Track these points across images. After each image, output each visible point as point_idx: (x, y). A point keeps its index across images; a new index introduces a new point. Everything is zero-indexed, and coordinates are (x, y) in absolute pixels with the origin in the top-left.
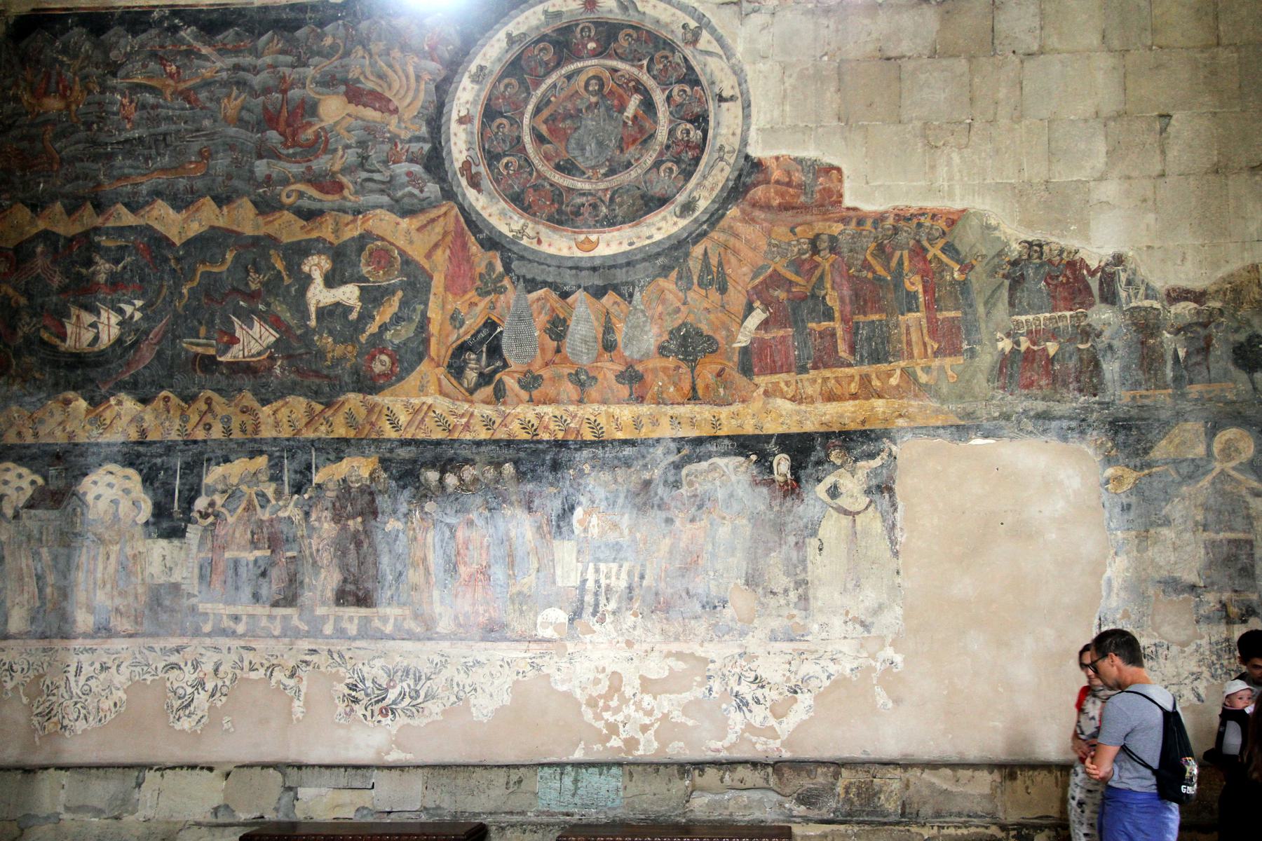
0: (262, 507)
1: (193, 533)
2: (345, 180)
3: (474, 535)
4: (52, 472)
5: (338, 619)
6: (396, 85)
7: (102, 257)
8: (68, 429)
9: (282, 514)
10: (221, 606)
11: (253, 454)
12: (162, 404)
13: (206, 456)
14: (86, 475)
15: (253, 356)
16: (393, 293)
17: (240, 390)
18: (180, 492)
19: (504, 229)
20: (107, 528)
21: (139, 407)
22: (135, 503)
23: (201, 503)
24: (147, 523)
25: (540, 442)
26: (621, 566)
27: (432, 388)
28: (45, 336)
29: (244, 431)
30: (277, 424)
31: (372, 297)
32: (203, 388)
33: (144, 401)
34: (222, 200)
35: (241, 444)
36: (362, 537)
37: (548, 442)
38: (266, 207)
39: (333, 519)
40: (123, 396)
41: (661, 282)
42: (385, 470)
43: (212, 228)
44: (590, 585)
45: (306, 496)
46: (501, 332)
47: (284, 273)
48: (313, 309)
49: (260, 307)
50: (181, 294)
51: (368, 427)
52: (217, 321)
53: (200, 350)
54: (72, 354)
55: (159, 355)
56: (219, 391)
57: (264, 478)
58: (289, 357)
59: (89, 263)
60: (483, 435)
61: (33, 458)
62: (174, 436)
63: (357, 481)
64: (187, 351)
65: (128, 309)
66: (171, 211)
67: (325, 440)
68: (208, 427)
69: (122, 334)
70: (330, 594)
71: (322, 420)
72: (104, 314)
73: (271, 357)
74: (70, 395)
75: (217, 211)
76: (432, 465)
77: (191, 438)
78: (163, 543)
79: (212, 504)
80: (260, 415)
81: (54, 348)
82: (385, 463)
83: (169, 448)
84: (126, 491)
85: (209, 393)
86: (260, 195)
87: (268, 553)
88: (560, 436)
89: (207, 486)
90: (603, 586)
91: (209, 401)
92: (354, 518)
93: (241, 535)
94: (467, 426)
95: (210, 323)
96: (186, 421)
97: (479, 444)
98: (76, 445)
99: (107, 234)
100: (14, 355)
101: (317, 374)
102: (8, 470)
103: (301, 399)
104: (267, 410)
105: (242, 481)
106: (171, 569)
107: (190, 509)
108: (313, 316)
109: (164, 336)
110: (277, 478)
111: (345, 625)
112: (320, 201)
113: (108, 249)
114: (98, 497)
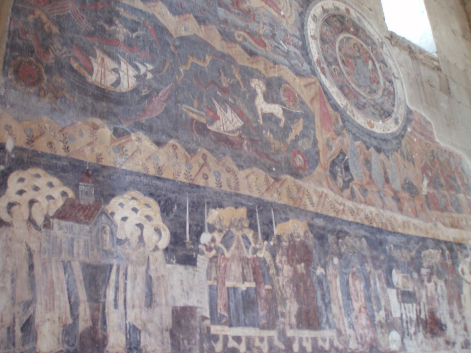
0: (247, 248)
1: (202, 261)
2: (266, 41)
3: (357, 283)
4: (82, 187)
5: (301, 340)
6: (282, 5)
7: (120, 22)
8: (97, 151)
9: (261, 255)
10: (226, 328)
11: (237, 205)
12: (171, 150)
13: (206, 200)
14: (113, 196)
15: (229, 132)
16: (299, 118)
17: (224, 155)
18: (190, 226)
19: (339, 102)
20: (133, 250)
21: (154, 148)
22: (158, 231)
23: (205, 238)
24: (166, 250)
25: (373, 227)
26: (413, 306)
27: (325, 184)
28: (75, 65)
29: (230, 186)
30: (250, 186)
31: (290, 116)
32: (199, 145)
33: (159, 144)
34: (201, 21)
35: (230, 195)
36: (305, 278)
37: (376, 228)
38: (227, 37)
39: (288, 263)
40: (141, 134)
41: (396, 153)
42: (312, 232)
43: (195, 35)
44: (404, 317)
45: (272, 243)
46: (348, 159)
47: (241, 83)
48: (260, 113)
49: (230, 100)
50: (179, 73)
51: (299, 200)
52: (205, 100)
53: (195, 116)
54: (97, 88)
55: (167, 111)
56: (212, 151)
57: (246, 225)
58: (252, 140)
59: (111, 22)
60: (351, 219)
61: (64, 169)
62: (182, 178)
63: (298, 237)
64: (186, 115)
65: (143, 70)
66: (169, 13)
67: (278, 204)
68: (206, 177)
69: (138, 85)
70: (294, 320)
71: (274, 190)
72: (124, 66)
73: (240, 136)
74: (98, 121)
75: (198, 26)
76: (332, 231)
77: (196, 183)
78: (180, 268)
79: (213, 240)
80: (238, 176)
81: (84, 77)
82: (311, 226)
83: (181, 188)
84: (148, 217)
85: (205, 151)
86: (222, 28)
87: (253, 285)
88: (380, 226)
89: (208, 224)
90: (409, 318)
91: (204, 157)
92: (300, 263)
93: (235, 269)
94: (343, 211)
95: (200, 99)
96: (190, 169)
97: (350, 223)
98: (104, 167)
99: (124, 8)
100: (46, 72)
101: (267, 156)
102: (38, 176)
103: (261, 171)
104: (242, 174)
105: (232, 224)
106: (188, 294)
107: (198, 241)
108: (261, 117)
109: (169, 97)
110: (253, 226)
111: (305, 344)
112: (255, 47)
113: (125, 19)
114: (124, 219)
